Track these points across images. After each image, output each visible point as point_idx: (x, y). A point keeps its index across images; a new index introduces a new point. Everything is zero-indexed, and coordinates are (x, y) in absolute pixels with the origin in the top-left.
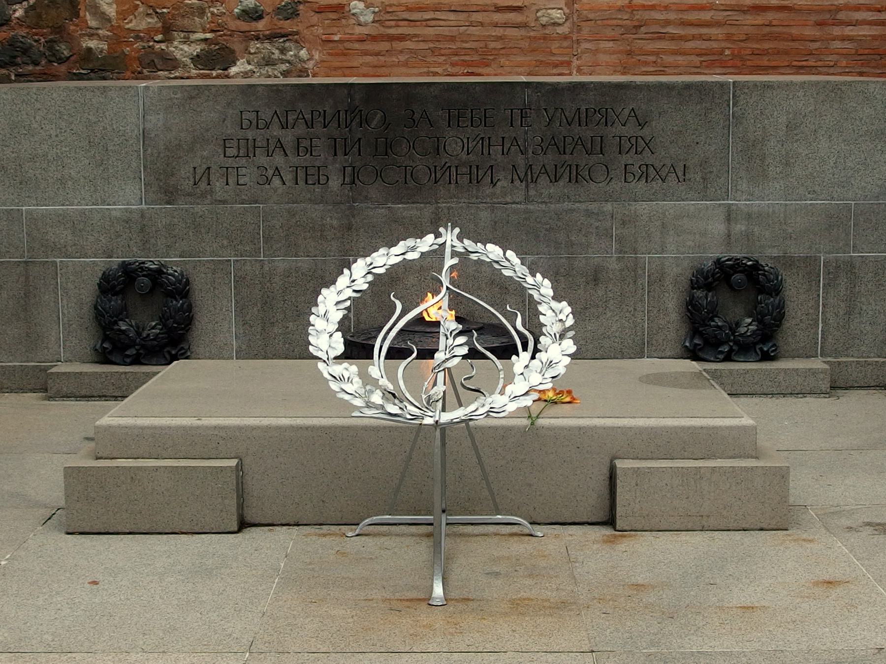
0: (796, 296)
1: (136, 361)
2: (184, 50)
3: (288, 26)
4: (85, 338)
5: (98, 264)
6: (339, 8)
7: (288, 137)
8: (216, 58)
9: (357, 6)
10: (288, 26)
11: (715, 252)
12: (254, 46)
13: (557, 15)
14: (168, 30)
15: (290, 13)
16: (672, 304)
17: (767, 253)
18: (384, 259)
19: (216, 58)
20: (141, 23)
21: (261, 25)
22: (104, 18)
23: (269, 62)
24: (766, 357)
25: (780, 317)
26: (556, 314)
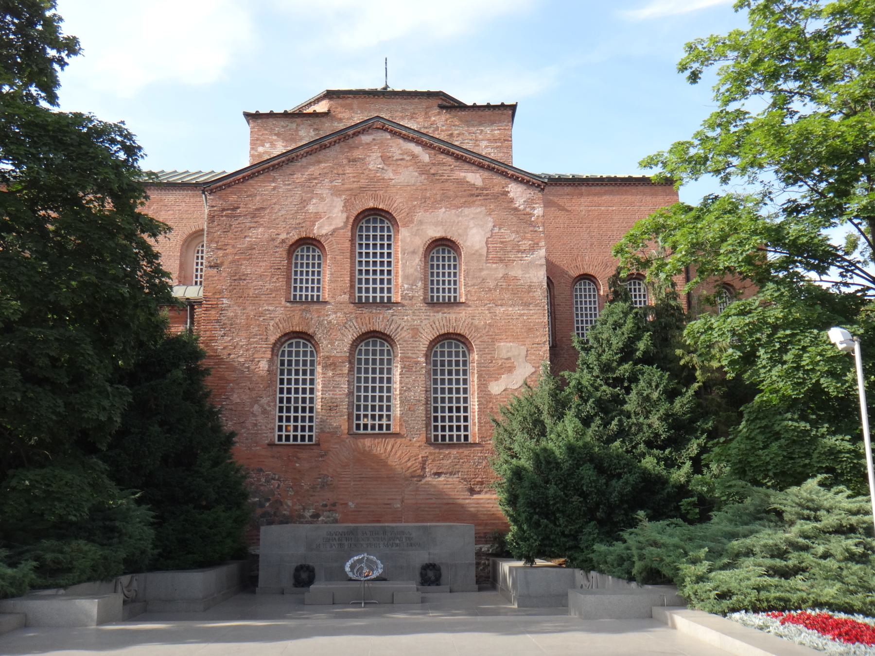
0: (444, 572)
1: (303, 586)
2: (308, 514)
3: (334, 508)
4: (292, 581)
5: (294, 565)
6: (346, 504)
7: (337, 537)
8: (316, 516)
9: (350, 504)
10: (334, 508)
11: (427, 562)
12: (325, 513)
13: (399, 506)
14: (304, 509)
15: (334, 505)
16: (417, 573)
17: (437, 562)
18: (356, 558)
19: (316, 516)
20: (297, 507)
21: (327, 508)
22: (288, 506)
23: (328, 517)
24: (437, 585)
25: (440, 576)
26: (380, 565)
